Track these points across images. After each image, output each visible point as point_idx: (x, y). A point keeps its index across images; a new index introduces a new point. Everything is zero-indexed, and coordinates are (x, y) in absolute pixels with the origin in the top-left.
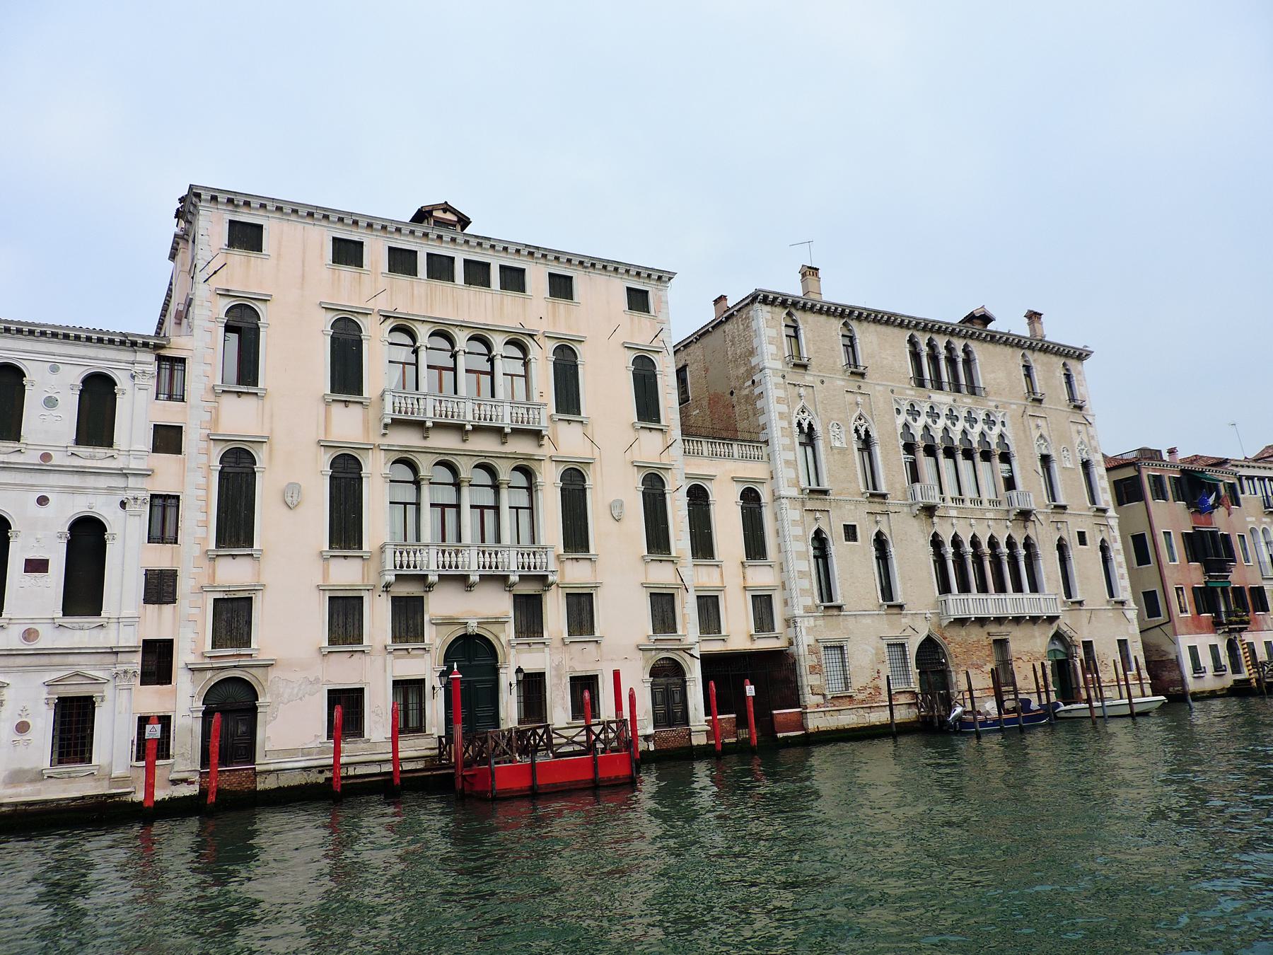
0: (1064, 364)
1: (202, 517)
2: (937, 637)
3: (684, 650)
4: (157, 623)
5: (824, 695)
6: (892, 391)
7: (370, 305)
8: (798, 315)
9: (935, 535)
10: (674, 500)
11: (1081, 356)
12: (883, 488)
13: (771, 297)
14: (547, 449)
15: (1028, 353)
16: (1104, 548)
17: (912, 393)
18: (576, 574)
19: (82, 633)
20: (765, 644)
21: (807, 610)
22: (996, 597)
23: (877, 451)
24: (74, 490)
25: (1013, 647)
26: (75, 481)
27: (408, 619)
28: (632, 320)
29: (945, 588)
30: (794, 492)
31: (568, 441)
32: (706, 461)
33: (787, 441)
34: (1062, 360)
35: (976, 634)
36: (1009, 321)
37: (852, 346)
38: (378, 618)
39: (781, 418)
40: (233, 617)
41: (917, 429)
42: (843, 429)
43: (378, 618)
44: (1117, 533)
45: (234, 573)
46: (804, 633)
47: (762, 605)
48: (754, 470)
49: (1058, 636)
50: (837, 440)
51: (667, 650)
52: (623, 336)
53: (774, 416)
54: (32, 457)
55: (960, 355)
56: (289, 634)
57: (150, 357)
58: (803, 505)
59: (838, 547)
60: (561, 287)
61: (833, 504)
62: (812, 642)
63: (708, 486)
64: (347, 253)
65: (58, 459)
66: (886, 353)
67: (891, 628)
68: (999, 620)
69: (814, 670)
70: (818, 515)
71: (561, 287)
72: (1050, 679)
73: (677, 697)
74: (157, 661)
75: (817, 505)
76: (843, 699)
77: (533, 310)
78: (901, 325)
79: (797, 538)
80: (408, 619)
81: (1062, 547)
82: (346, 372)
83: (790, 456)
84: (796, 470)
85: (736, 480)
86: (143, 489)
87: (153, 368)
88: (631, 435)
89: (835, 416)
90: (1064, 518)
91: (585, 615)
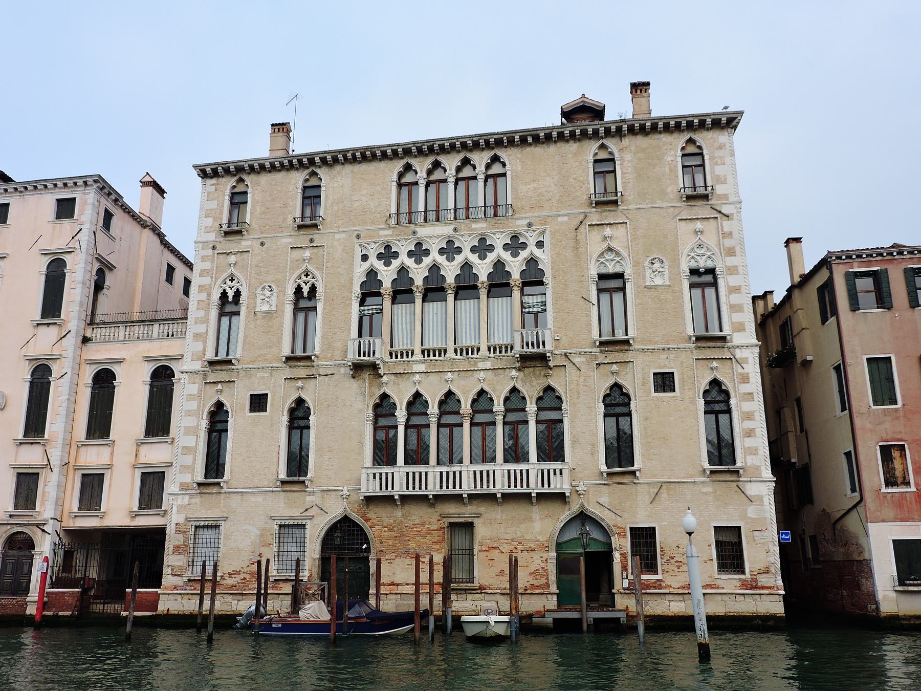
2: (355, 517)
3: (37, 525)
6: (358, 237)
10: (57, 387)
11: (726, 122)
12: (317, 348)
13: (672, 123)
21: (184, 487)
28: (54, 228)
32: (119, 345)
33: (202, 313)
35: (418, 515)
36: (619, 107)
39: (200, 291)
41: (387, 275)
42: (275, 290)
44: (753, 369)
46: (177, 511)
48: (162, 348)
49: (583, 517)
51: (20, 525)
52: (44, 245)
58: (204, 379)
61: (242, 374)
62: (181, 520)
63: (116, 369)
67: (286, 507)
69: (177, 550)
70: (220, 386)
75: (223, 376)
79: (189, 413)
83: (201, 329)
84: (205, 342)
85: (148, 360)
88: (31, 331)
90: (628, 356)
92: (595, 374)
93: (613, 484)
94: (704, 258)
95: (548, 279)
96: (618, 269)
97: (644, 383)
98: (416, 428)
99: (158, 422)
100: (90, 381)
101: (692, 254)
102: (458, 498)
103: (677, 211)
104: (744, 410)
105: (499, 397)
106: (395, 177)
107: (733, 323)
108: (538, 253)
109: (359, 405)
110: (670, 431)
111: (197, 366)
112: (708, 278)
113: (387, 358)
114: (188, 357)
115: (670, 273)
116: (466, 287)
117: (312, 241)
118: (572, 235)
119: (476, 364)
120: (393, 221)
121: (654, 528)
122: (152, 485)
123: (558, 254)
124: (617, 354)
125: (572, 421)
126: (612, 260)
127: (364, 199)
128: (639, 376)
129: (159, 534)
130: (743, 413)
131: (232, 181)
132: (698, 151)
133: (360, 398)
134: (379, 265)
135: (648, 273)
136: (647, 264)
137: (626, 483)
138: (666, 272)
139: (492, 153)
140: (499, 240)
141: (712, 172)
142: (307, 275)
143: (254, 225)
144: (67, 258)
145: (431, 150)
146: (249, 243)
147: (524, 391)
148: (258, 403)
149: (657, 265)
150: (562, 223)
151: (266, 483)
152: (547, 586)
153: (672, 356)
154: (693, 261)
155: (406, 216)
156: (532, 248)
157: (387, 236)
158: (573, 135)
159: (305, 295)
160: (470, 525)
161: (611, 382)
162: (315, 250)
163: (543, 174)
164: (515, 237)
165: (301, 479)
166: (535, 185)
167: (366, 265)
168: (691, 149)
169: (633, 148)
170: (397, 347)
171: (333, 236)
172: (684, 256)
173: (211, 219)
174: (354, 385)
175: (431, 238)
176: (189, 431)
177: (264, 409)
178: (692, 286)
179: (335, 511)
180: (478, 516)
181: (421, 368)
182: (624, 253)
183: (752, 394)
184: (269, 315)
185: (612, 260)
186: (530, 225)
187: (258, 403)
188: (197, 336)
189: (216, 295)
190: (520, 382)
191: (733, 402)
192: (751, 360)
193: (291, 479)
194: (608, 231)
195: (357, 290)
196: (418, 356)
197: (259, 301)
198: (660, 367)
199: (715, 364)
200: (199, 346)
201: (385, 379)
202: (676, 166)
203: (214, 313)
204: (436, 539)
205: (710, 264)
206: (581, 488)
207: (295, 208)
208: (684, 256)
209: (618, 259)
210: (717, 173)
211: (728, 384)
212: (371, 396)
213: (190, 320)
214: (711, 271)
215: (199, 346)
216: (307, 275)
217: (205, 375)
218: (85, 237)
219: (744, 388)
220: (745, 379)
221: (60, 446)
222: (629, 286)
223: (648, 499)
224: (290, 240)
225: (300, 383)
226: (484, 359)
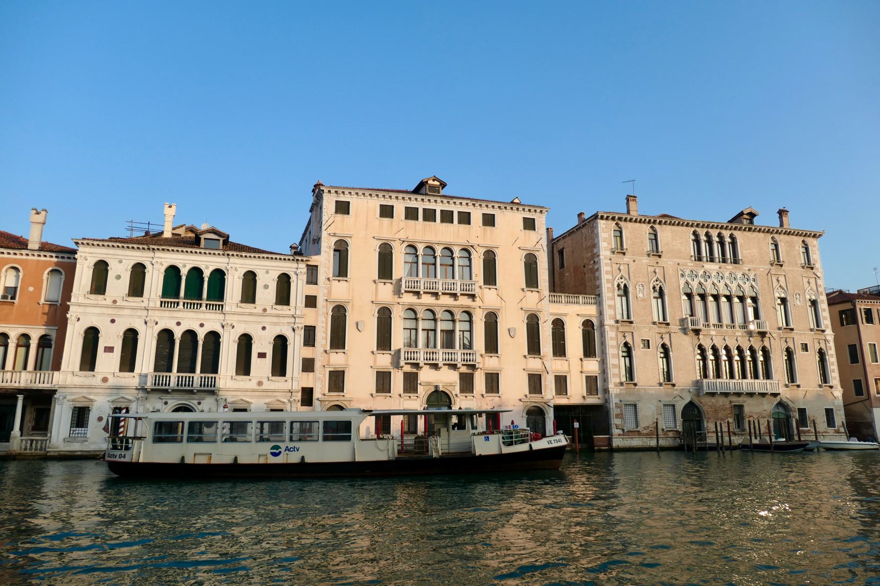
0: (803, 241)
1: (324, 335)
2: (696, 401)
4: (307, 380)
5: (623, 430)
7: (397, 236)
8: (622, 224)
9: (700, 347)
14: (478, 302)
15: (776, 236)
16: (822, 354)
17: (691, 264)
18: (490, 363)
19: (279, 383)
20: (592, 400)
23: (666, 298)
24: (276, 324)
26: (275, 320)
27: (411, 383)
30: (612, 322)
31: (488, 298)
33: (610, 295)
34: (802, 238)
35: (722, 401)
37: (656, 239)
38: (397, 381)
40: (337, 380)
43: (397, 381)
44: (832, 344)
45: (337, 359)
47: (591, 382)
48: (590, 311)
49: (781, 404)
50: (641, 293)
53: (604, 281)
55: (728, 240)
56: (360, 390)
59: (638, 353)
60: (489, 220)
62: (618, 401)
63: (564, 319)
64: (387, 212)
65: (269, 311)
66: (677, 242)
68: (739, 394)
71: (489, 220)
72: (772, 429)
73: (540, 426)
74: (307, 396)
76: (627, 433)
77: (475, 234)
78: (687, 225)
80: (411, 383)
81: (790, 353)
82: (385, 269)
83: (612, 303)
86: (301, 323)
87: (305, 270)
89: (641, 280)
91: (495, 384)
108: (754, 284)
120: (693, 259)
145: (708, 227)
171: (667, 261)
179: (687, 401)
184: (643, 300)
200: (612, 312)
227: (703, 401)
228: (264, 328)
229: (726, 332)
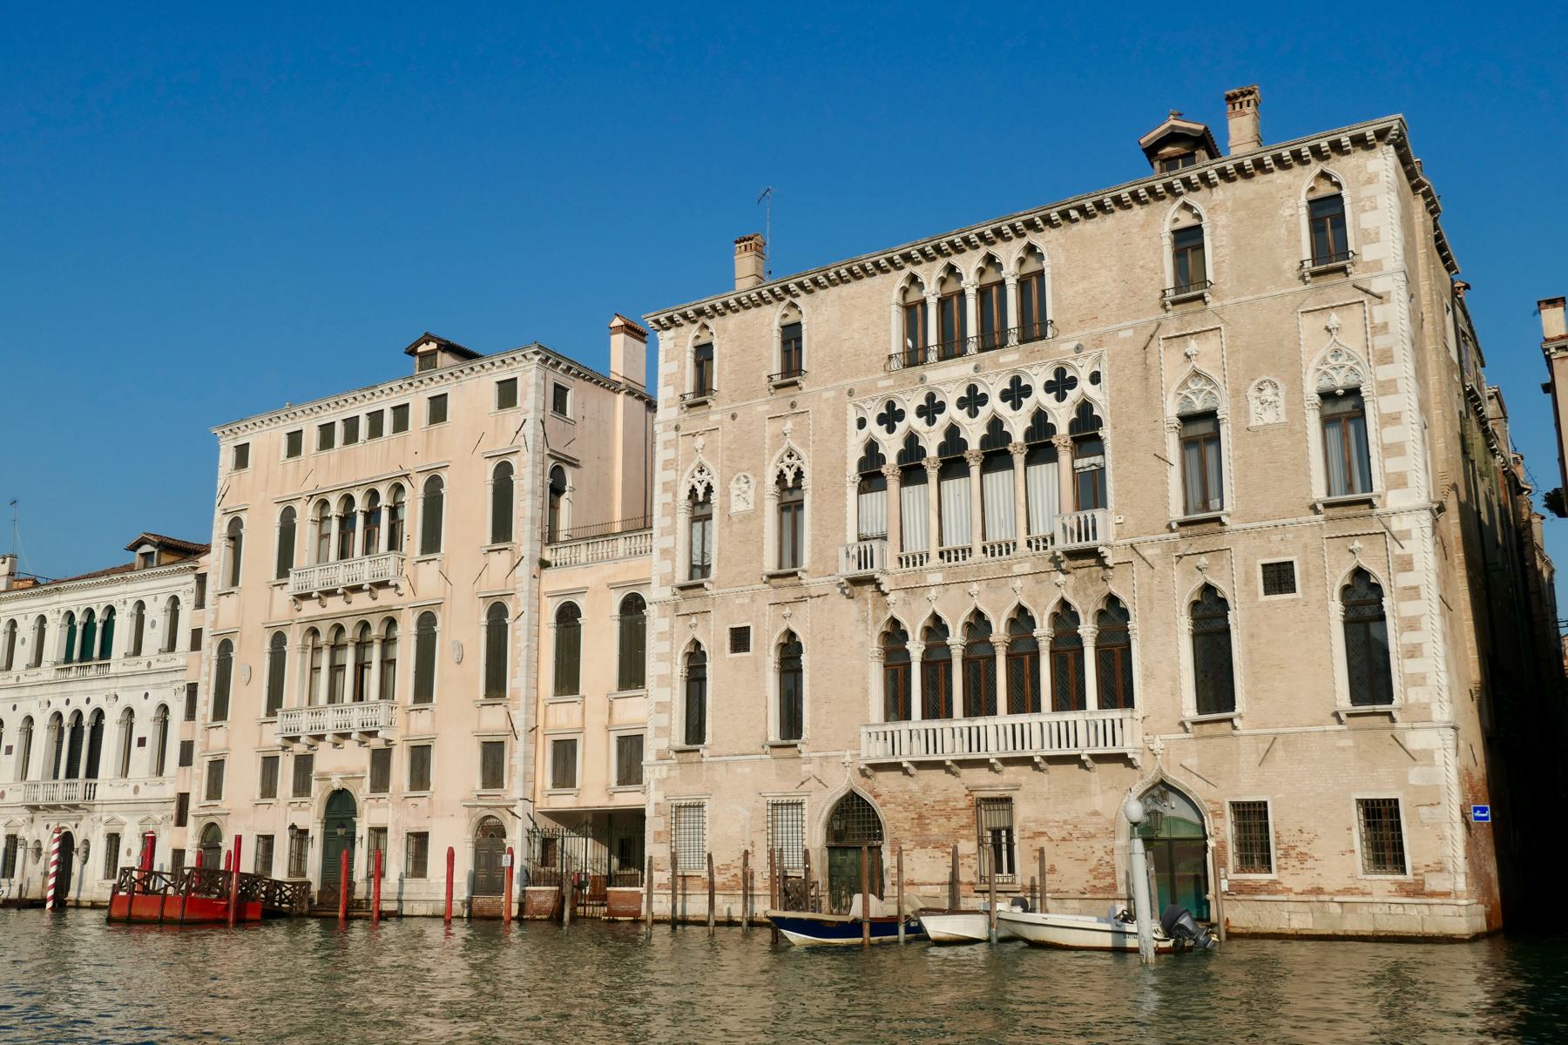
3: (507, 808)
22: (966, 723)
24: (158, 686)
25: (1024, 813)
29: (897, 707)
32: (579, 569)
33: (668, 521)
39: (665, 491)
41: (891, 447)
49: (1163, 788)
52: (487, 447)
54: (143, 667)
57: (191, 578)
58: (676, 610)
62: (661, 799)
63: (581, 602)
70: (694, 620)
75: (697, 605)
83: (668, 542)
84: (673, 561)
88: (482, 560)
92: (1177, 572)
93: (1204, 737)
94: (1343, 371)
95: (1105, 432)
96: (1209, 405)
97: (1248, 581)
98: (936, 666)
99: (632, 673)
100: (552, 619)
101: (1324, 368)
102: (984, 763)
103: (1299, 299)
104: (1403, 614)
105: (1042, 615)
106: (896, 296)
107: (1387, 475)
109: (861, 637)
110: (1285, 655)
111: (666, 593)
112: (1347, 406)
113: (892, 565)
114: (655, 581)
115: (1288, 402)
116: (996, 455)
117: (793, 405)
118: (1138, 359)
119: (1009, 568)
120: (895, 364)
121: (1265, 804)
122: (630, 750)
123: (1120, 390)
124: (1206, 539)
125: (1143, 646)
126: (1201, 391)
127: (857, 336)
128: (1238, 570)
129: (637, 816)
130: (1403, 619)
131: (693, 330)
132: (1335, 190)
133: (862, 627)
134: (879, 432)
135: (1254, 405)
136: (1252, 392)
137: (1222, 736)
138: (1281, 402)
139: (1024, 242)
140: (1038, 377)
141: (1357, 226)
142: (790, 456)
143: (723, 391)
144: (513, 460)
146: (718, 417)
147: (1076, 605)
148: (740, 640)
149: (1269, 391)
150: (1125, 340)
151: (753, 749)
152: (1113, 887)
153: (1289, 536)
154: (1325, 378)
155: (914, 358)
156: (1084, 385)
157: (887, 388)
158: (1135, 196)
159: (790, 484)
160: (1008, 800)
161: (1200, 583)
162: (799, 418)
163: (1096, 266)
164: (1060, 372)
165: (793, 742)
166: (1086, 284)
167: (864, 433)
168: (1325, 189)
169: (1229, 204)
170: (907, 551)
172: (1311, 372)
173: (671, 388)
174: (852, 607)
175: (944, 384)
176: (665, 680)
177: (747, 649)
178: (1327, 421)
180: (1017, 788)
181: (937, 578)
182: (1217, 377)
183: (1416, 588)
184: (746, 517)
185: (1201, 391)
186: (1078, 349)
187: (740, 640)
188: (665, 553)
189: (684, 493)
190: (1070, 591)
191: (1386, 602)
192: (1416, 533)
193: (785, 742)
194: (1193, 346)
195: (853, 470)
196: (935, 559)
197: (733, 497)
198: (1271, 555)
199: (1357, 544)
200: (666, 567)
201: (891, 598)
202: (1298, 224)
203: (683, 519)
204: (964, 821)
205: (1352, 381)
206: (1157, 745)
207: (770, 359)
208: (1311, 372)
209: (1208, 388)
210: (1363, 226)
211: (1379, 575)
212: (875, 623)
213: (656, 531)
214: (1354, 393)
215: (666, 567)
216: (790, 456)
217: (676, 607)
218: (528, 430)
219: (1404, 579)
220: (1407, 565)
221: (522, 707)
222: (1225, 432)
223: (1255, 759)
224: (767, 407)
225: (787, 611)
226: (1021, 560)
227: (881, 790)
228: (146, 695)
229: (979, 567)
